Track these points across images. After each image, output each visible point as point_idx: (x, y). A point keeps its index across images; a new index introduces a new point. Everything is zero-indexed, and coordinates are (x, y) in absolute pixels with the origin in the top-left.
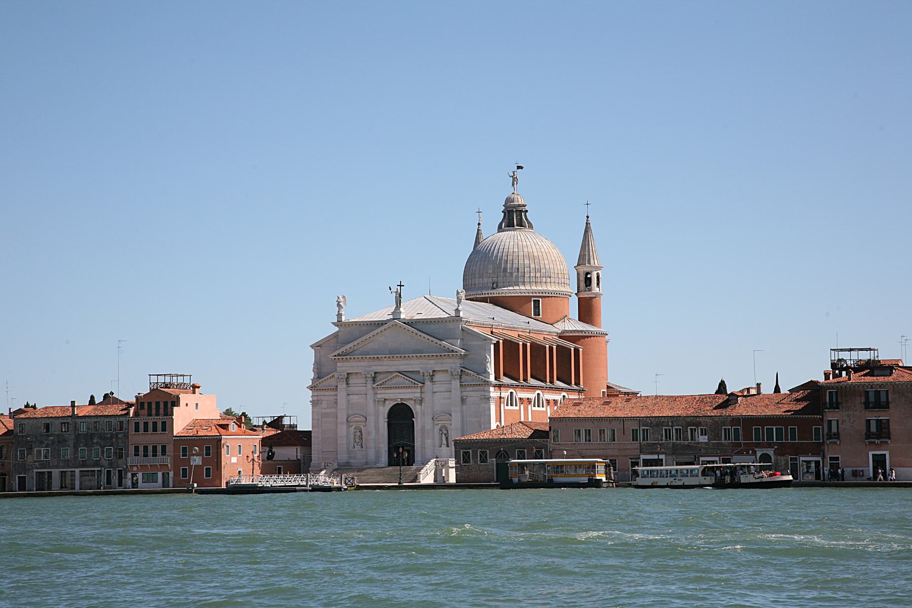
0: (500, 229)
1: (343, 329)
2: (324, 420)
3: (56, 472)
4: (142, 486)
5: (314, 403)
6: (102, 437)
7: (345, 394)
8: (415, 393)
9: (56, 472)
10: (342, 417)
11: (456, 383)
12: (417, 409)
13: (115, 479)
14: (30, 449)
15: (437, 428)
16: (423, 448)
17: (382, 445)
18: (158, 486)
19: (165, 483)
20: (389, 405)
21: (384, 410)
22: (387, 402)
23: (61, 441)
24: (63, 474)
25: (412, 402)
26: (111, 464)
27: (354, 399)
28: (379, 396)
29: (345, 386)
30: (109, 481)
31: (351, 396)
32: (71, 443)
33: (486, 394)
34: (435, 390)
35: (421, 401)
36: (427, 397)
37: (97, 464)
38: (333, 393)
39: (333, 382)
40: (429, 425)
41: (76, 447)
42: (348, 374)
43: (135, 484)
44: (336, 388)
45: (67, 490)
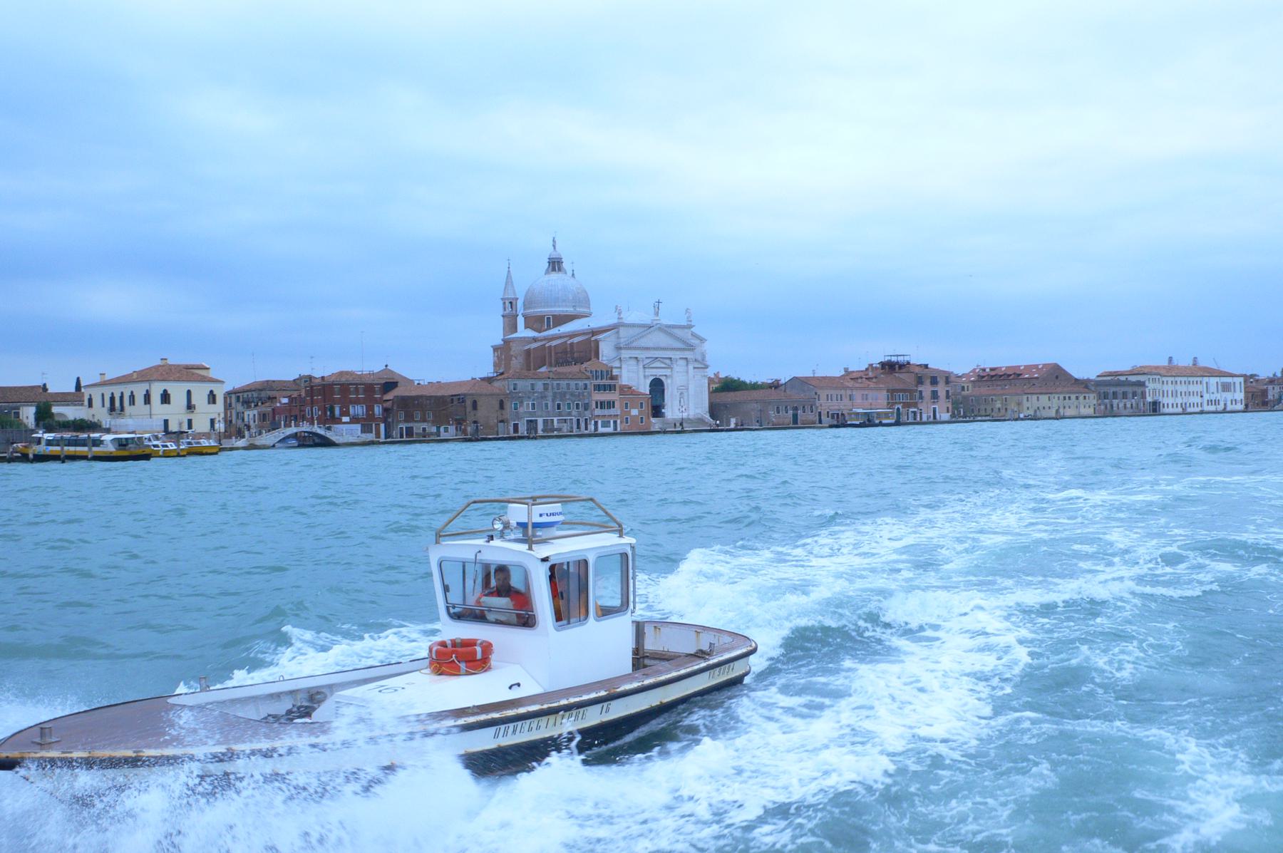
0: (547, 272)
3: (540, 421)
4: (601, 430)
6: (572, 395)
8: (668, 372)
9: (540, 421)
12: (667, 382)
13: (583, 425)
14: (522, 402)
18: (610, 430)
19: (615, 428)
21: (648, 382)
23: (544, 397)
24: (545, 422)
26: (580, 414)
30: (578, 427)
32: (550, 398)
35: (671, 376)
37: (570, 414)
41: (553, 401)
43: (596, 429)
45: (551, 433)
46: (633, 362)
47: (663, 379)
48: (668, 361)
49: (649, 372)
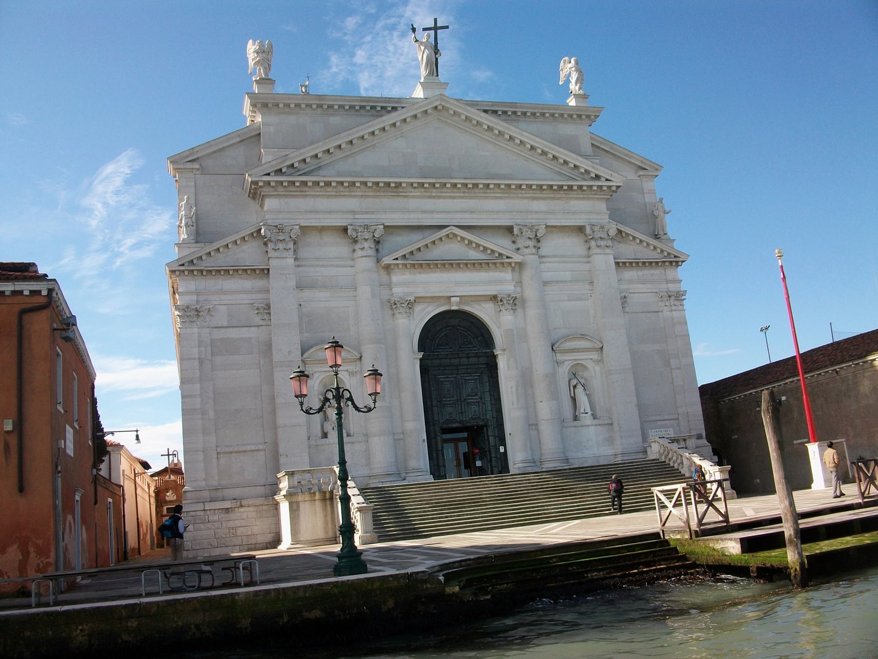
1: (273, 119)
2: (219, 359)
5: (190, 314)
7: (293, 283)
8: (502, 282)
10: (287, 347)
11: (604, 260)
15: (563, 371)
16: (532, 425)
17: (410, 426)
20: (425, 313)
21: (412, 326)
22: (418, 308)
25: (490, 306)
27: (320, 301)
28: (398, 291)
29: (291, 261)
31: (307, 294)
33: (672, 287)
34: (547, 276)
36: (530, 292)
38: (248, 283)
39: (249, 254)
40: (540, 364)
42: (304, 229)
44: (265, 272)
46: (336, 248)
47: (484, 312)
48: (500, 244)
49: (405, 284)
